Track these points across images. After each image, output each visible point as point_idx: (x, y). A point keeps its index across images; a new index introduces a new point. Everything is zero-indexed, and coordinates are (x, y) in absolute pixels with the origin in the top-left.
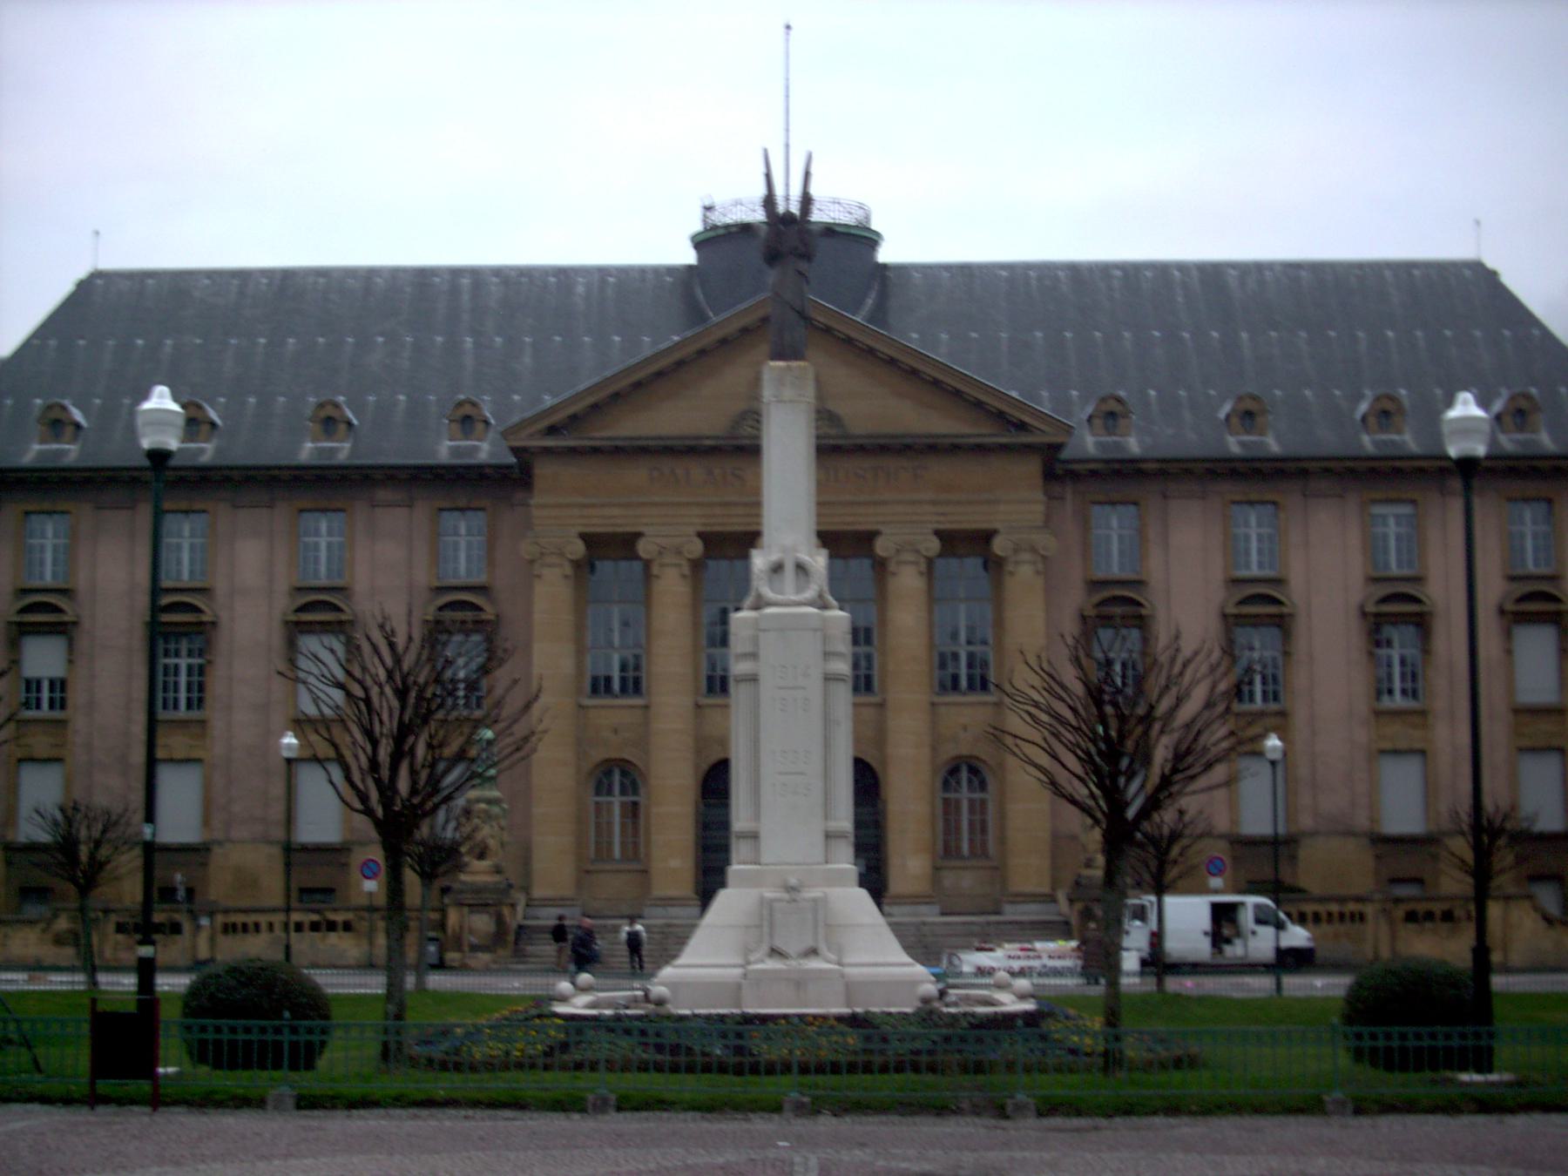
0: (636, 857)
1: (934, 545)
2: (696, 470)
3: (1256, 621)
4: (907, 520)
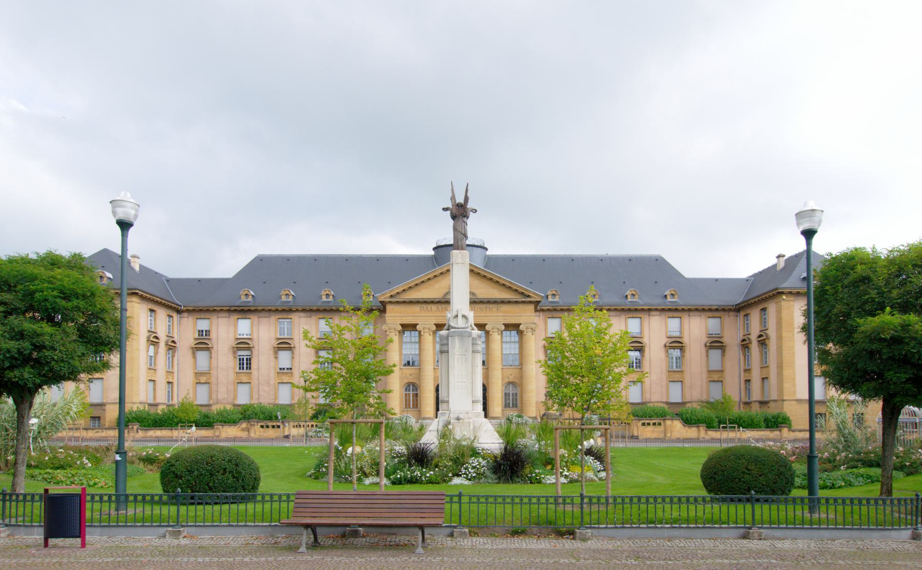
0: (417, 407)
1: (503, 327)
2: (434, 307)
3: (674, 348)
4: (496, 318)
